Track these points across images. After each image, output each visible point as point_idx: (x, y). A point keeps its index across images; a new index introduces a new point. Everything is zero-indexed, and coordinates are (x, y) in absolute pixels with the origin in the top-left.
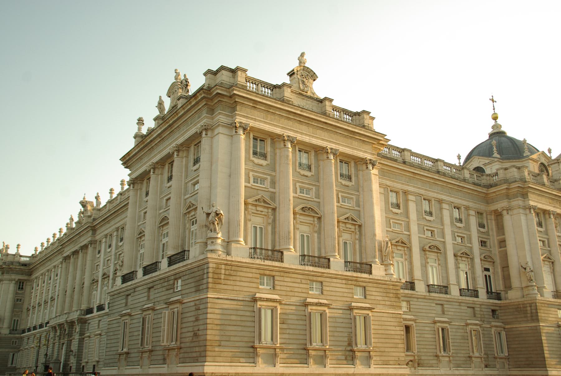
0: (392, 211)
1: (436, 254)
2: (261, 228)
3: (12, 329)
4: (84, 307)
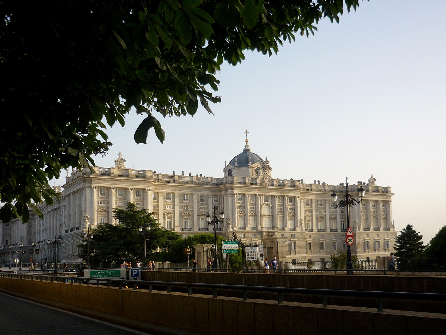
0: (166, 202)
1: (188, 216)
2: (103, 218)
3: (28, 242)
4: (58, 236)
